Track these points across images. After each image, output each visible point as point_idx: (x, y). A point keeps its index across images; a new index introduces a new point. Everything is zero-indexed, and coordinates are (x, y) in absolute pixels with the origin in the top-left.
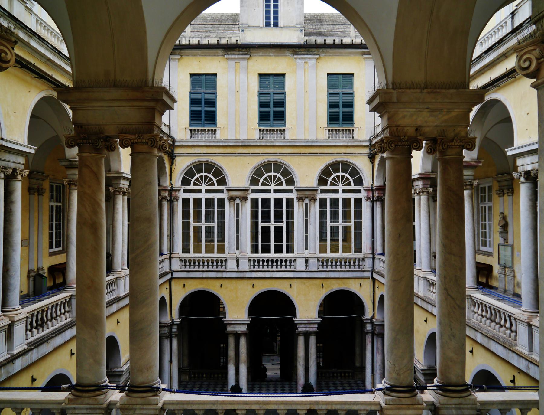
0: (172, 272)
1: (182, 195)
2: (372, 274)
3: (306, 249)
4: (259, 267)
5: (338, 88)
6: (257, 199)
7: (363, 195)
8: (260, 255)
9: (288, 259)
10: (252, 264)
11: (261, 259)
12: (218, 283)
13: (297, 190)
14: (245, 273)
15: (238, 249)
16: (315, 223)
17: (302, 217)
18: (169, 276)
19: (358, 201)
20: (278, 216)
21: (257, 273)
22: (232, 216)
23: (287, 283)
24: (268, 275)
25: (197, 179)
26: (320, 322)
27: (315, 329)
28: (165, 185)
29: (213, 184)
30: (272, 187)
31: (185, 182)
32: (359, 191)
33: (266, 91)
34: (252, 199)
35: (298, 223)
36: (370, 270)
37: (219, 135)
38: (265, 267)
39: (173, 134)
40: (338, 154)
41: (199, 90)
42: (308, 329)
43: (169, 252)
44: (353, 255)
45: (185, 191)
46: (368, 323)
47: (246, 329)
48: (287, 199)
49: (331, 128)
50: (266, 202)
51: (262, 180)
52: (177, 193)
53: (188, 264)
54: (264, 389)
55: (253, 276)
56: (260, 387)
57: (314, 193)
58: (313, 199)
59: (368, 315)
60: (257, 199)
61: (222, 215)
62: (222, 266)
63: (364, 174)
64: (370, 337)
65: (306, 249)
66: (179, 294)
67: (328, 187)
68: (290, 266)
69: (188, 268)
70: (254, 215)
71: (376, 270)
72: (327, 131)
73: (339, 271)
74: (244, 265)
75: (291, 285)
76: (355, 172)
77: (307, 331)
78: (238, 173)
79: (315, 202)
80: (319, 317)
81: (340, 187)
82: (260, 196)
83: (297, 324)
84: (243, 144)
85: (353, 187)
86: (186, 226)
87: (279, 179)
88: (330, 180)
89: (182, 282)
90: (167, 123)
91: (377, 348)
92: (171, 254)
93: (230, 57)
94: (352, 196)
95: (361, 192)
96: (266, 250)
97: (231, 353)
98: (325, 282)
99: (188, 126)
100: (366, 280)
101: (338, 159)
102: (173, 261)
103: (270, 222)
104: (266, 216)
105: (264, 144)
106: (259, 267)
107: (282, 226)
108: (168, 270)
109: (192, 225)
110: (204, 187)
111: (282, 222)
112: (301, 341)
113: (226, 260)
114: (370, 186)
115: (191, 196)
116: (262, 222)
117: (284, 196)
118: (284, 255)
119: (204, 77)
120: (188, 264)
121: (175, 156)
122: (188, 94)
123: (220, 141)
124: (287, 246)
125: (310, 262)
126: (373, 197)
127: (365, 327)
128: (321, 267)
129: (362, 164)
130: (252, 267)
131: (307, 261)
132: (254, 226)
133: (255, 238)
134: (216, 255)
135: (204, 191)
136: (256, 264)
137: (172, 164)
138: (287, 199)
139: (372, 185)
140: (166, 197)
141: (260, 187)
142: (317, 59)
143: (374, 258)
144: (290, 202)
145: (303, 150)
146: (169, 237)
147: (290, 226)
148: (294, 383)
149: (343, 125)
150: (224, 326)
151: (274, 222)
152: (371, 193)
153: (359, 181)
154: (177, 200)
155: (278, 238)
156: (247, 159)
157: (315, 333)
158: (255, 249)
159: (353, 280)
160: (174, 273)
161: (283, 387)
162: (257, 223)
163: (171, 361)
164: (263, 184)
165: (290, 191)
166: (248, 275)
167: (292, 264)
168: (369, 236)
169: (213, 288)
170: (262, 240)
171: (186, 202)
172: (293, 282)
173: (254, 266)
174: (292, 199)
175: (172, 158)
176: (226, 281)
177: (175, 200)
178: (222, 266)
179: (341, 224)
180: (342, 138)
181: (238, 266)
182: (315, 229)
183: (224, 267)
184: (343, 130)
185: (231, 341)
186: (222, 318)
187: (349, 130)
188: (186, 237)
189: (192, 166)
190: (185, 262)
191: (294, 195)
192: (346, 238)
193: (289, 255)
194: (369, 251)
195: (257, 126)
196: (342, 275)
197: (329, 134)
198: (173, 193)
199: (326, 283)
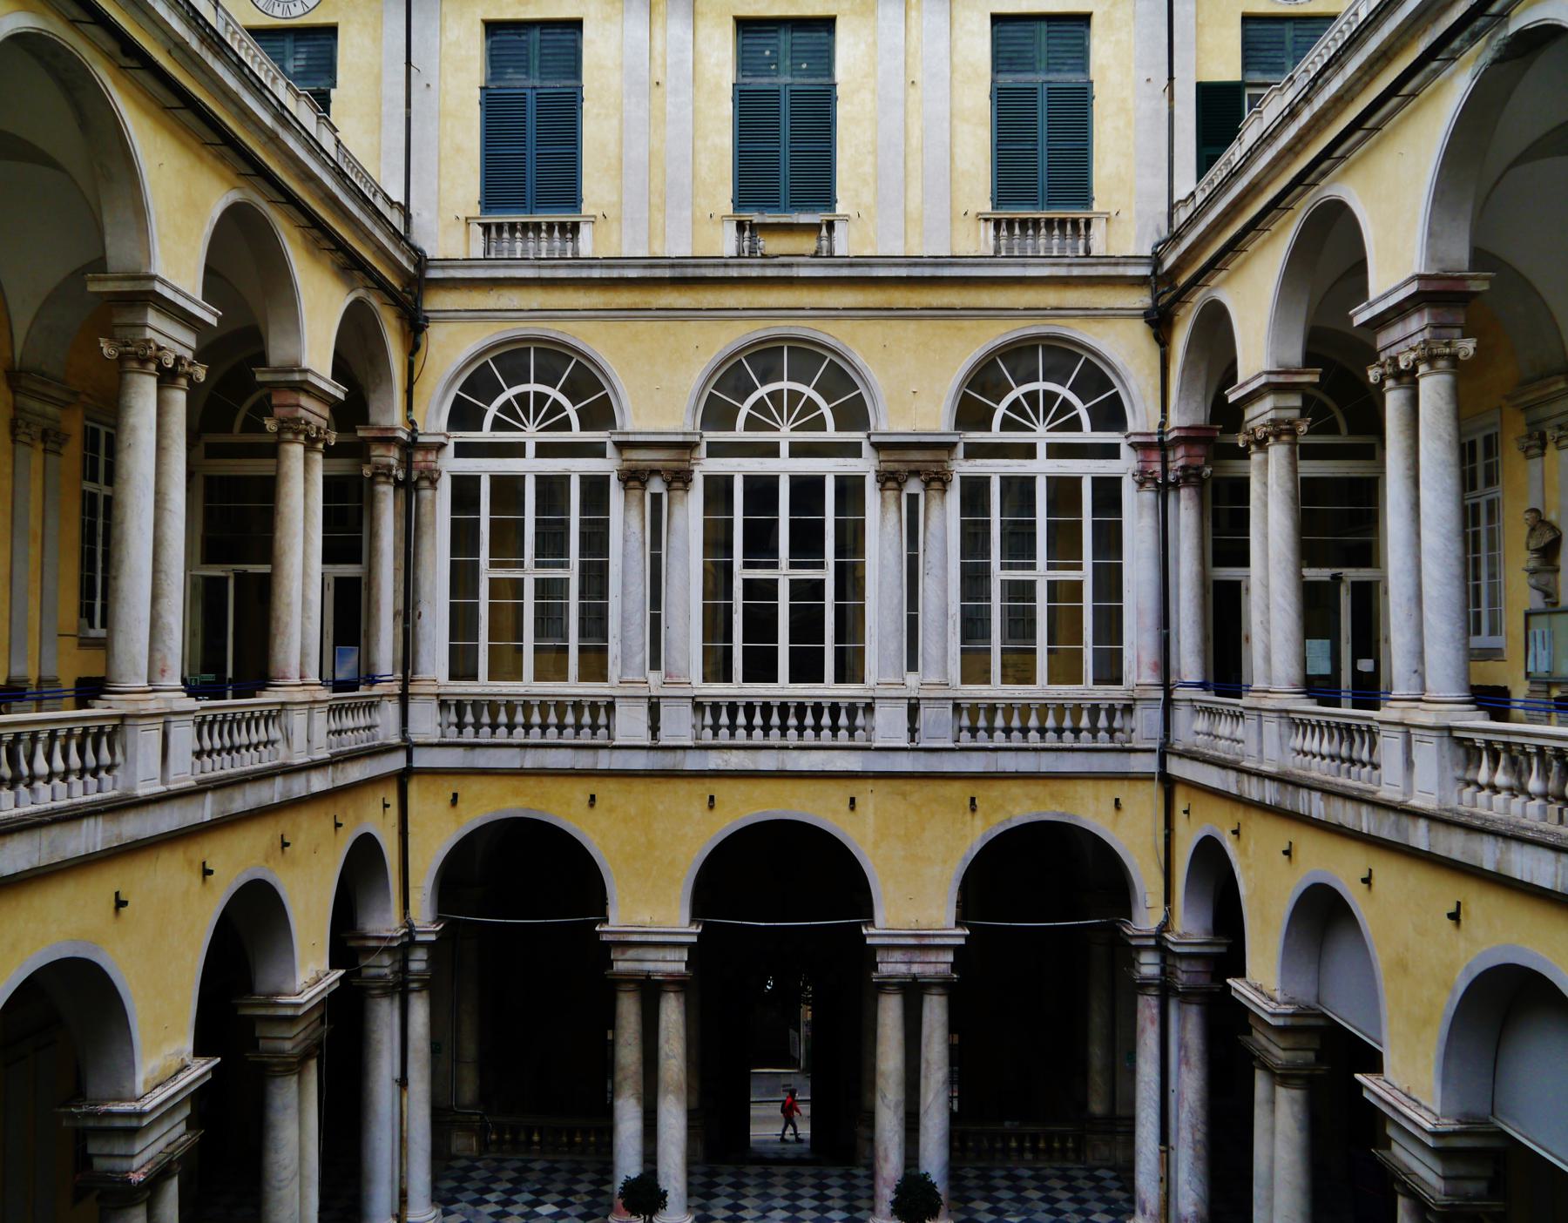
0: (408, 747)
1: (450, 465)
2: (1163, 763)
3: (912, 665)
4: (732, 735)
5: (1033, 71)
6: (729, 480)
7: (1125, 466)
8: (738, 688)
9: (843, 703)
10: (708, 720)
11: (741, 702)
12: (578, 791)
13: (878, 447)
14: (680, 753)
15: (655, 664)
16: (945, 569)
17: (895, 545)
18: (397, 762)
19: (1108, 491)
20: (807, 543)
21: (727, 755)
22: (635, 543)
23: (837, 793)
24: (766, 761)
25: (507, 408)
26: (962, 941)
27: (944, 969)
28: (385, 422)
29: (565, 425)
30: (785, 435)
31: (463, 416)
32: (1111, 452)
33: (763, 82)
34: (708, 479)
35: (882, 567)
36: (1155, 745)
37: (587, 244)
38: (758, 733)
39: (419, 238)
40: (1032, 311)
41: (517, 81)
42: (916, 969)
43: (399, 675)
44: (1087, 689)
45: (463, 450)
46: (1146, 948)
47: (682, 967)
48: (841, 481)
49: (1005, 213)
50: (761, 491)
51: (745, 409)
52: (431, 457)
53: (469, 718)
54: (752, 1191)
56: (738, 1185)
57: (943, 455)
58: (938, 480)
59: (1146, 918)
60: (729, 480)
61: (596, 539)
62: (594, 728)
63: (1133, 385)
64: (1154, 1002)
65: (912, 665)
67: (995, 435)
68: (852, 730)
69: (468, 735)
70: (716, 541)
71: (1179, 747)
72: (991, 225)
73: (1035, 750)
74: (679, 726)
75: (852, 800)
76: (1096, 380)
77: (915, 978)
78: (658, 380)
79: (944, 491)
81: (1041, 435)
82: (739, 468)
83: (874, 949)
84: (677, 273)
85: (1087, 435)
86: (463, 578)
87: (811, 405)
88: (1001, 410)
89: (449, 786)
90: (398, 196)
91: (1182, 1046)
92: (406, 682)
95: (1117, 456)
96: (761, 667)
97: (628, 1054)
98: (981, 791)
99: (475, 211)
100: (1140, 786)
101: (1033, 331)
102: (414, 708)
103: (775, 566)
104: (760, 544)
105: (754, 272)
106: (732, 735)
107: (823, 581)
108: (395, 740)
109: (486, 574)
110: (531, 435)
111: (821, 566)
112: (890, 1012)
113: (610, 707)
114: (1155, 429)
115: (485, 468)
116: (747, 565)
117: (829, 468)
118: (828, 689)
119: (536, 34)
120: (469, 718)
121: (427, 319)
122: (477, 94)
123: (592, 263)
124: (840, 654)
125: (925, 713)
126: (1165, 471)
127: (1132, 963)
128: (965, 735)
129: (1124, 347)
130: (709, 732)
131: (913, 710)
132: (717, 578)
133: (716, 623)
134: (573, 687)
135: (530, 449)
136: (724, 720)
137: (413, 347)
138: (841, 481)
139: (1162, 425)
140: (390, 467)
141: (739, 434)
143: (1168, 704)
144: (850, 490)
145: (899, 298)
146: (400, 620)
147: (850, 580)
148: (861, 1172)
149: (1051, 203)
150: (603, 951)
151: (793, 566)
152: (1155, 456)
153: (1111, 414)
154: (433, 483)
155: (807, 624)
156: (691, 331)
157: (945, 986)
158: (718, 668)
159: (1090, 783)
160: (416, 752)
161: (822, 1187)
162: (728, 568)
163: (403, 1082)
164: (751, 424)
165: (853, 450)
166: (692, 762)
167: (860, 721)
168: (1150, 618)
169: (563, 808)
170: (746, 635)
171: (465, 490)
173: (716, 728)
174: (860, 480)
175: (415, 327)
176: (611, 785)
177: (425, 484)
178: (594, 728)
179: (1041, 574)
180: (1045, 252)
181: (654, 728)
182: (945, 591)
183: (603, 731)
184: (1049, 222)
185: (628, 1009)
186: (595, 923)
187: (1075, 223)
188: (463, 622)
189: (488, 358)
190: (460, 713)
191: (865, 465)
192: (1064, 625)
193: (849, 690)
194: (1149, 677)
195: (728, 208)
196: (1047, 763)
197: (997, 237)
198: (419, 457)
199: (988, 794)
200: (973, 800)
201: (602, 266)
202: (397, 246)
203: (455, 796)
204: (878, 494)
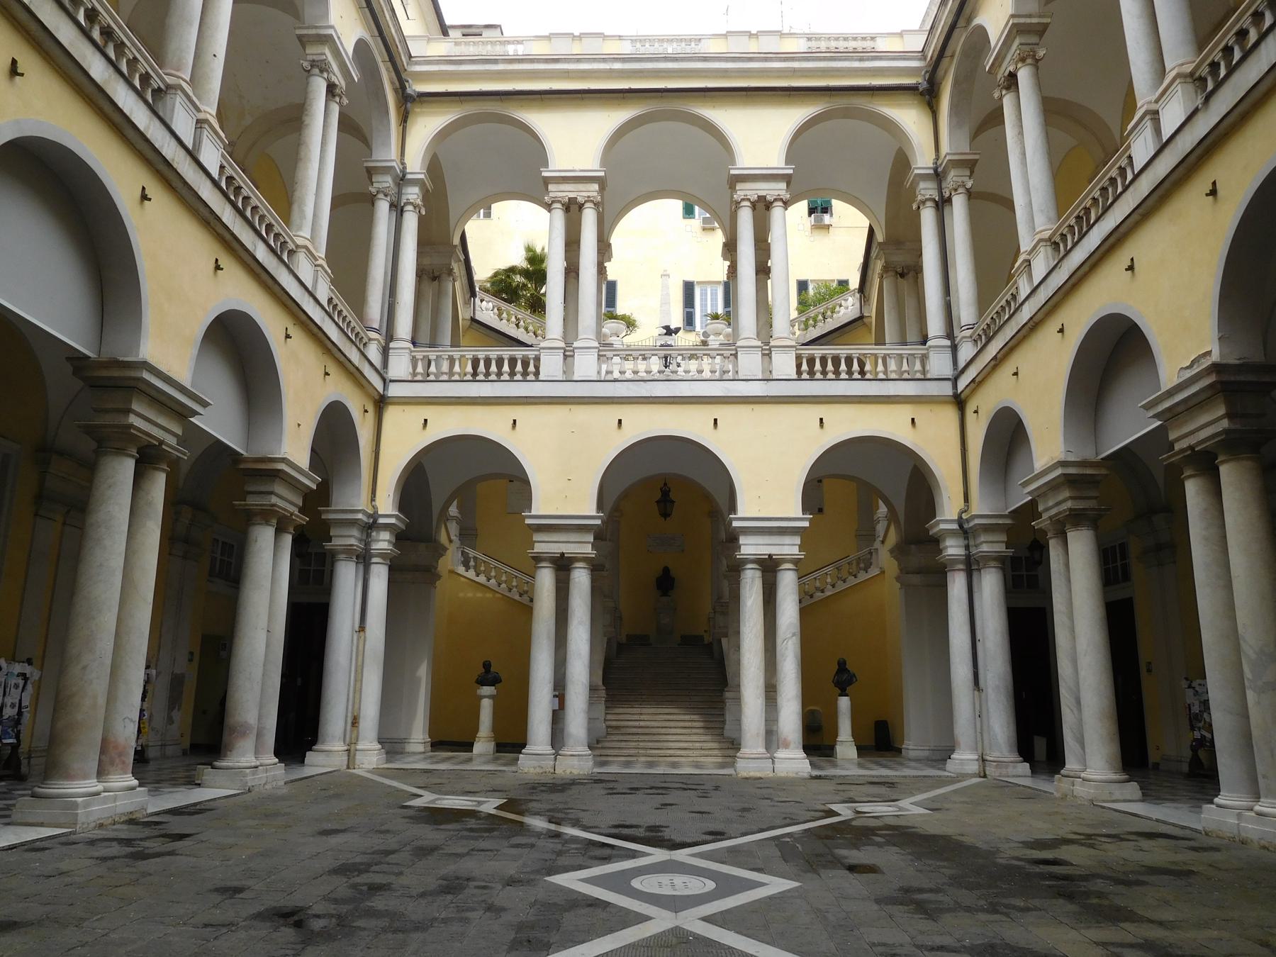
59: (949, 508)
66: (401, 439)
80: (804, 510)
139: (937, 157)
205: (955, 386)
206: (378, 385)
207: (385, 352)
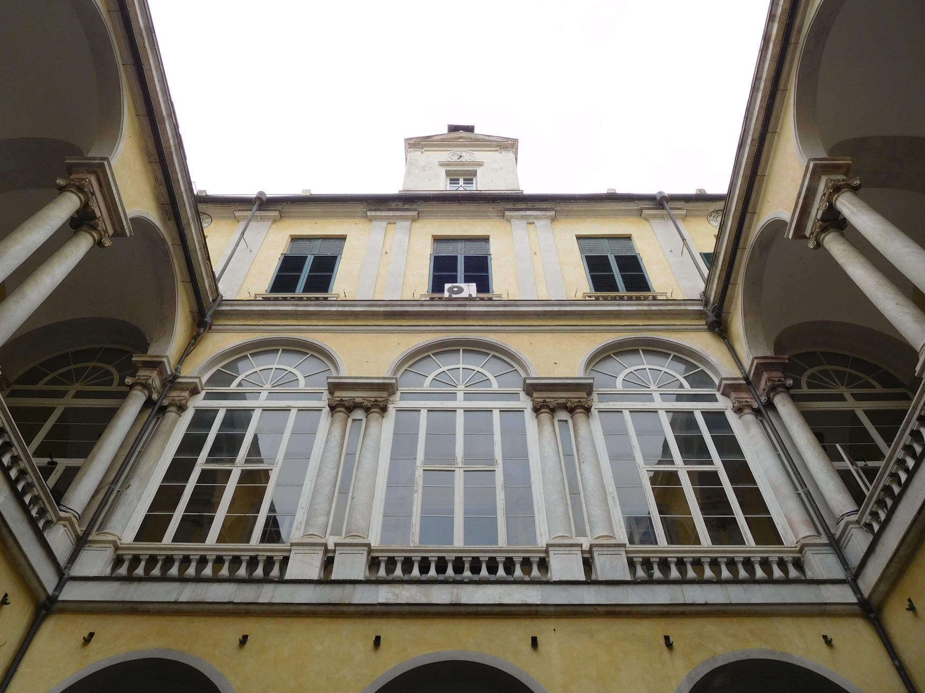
1: (200, 402)
12: (232, 630)
14: (348, 588)
35: (543, 458)
39: (221, 286)
52: (186, 394)
55: (382, 600)
86: (179, 469)
93: (378, 213)
94: (697, 408)
115: (223, 405)
142: (553, 219)
156: (395, 339)
159: (789, 621)
172: (545, 629)
176: (270, 625)
177: (173, 409)
188: (166, 498)
199: (683, 632)
200: (667, 638)
201: (339, 305)
202: (204, 262)
203: (91, 635)
204: (535, 421)
205: (857, 590)
206: (49, 579)
207: (81, 543)
